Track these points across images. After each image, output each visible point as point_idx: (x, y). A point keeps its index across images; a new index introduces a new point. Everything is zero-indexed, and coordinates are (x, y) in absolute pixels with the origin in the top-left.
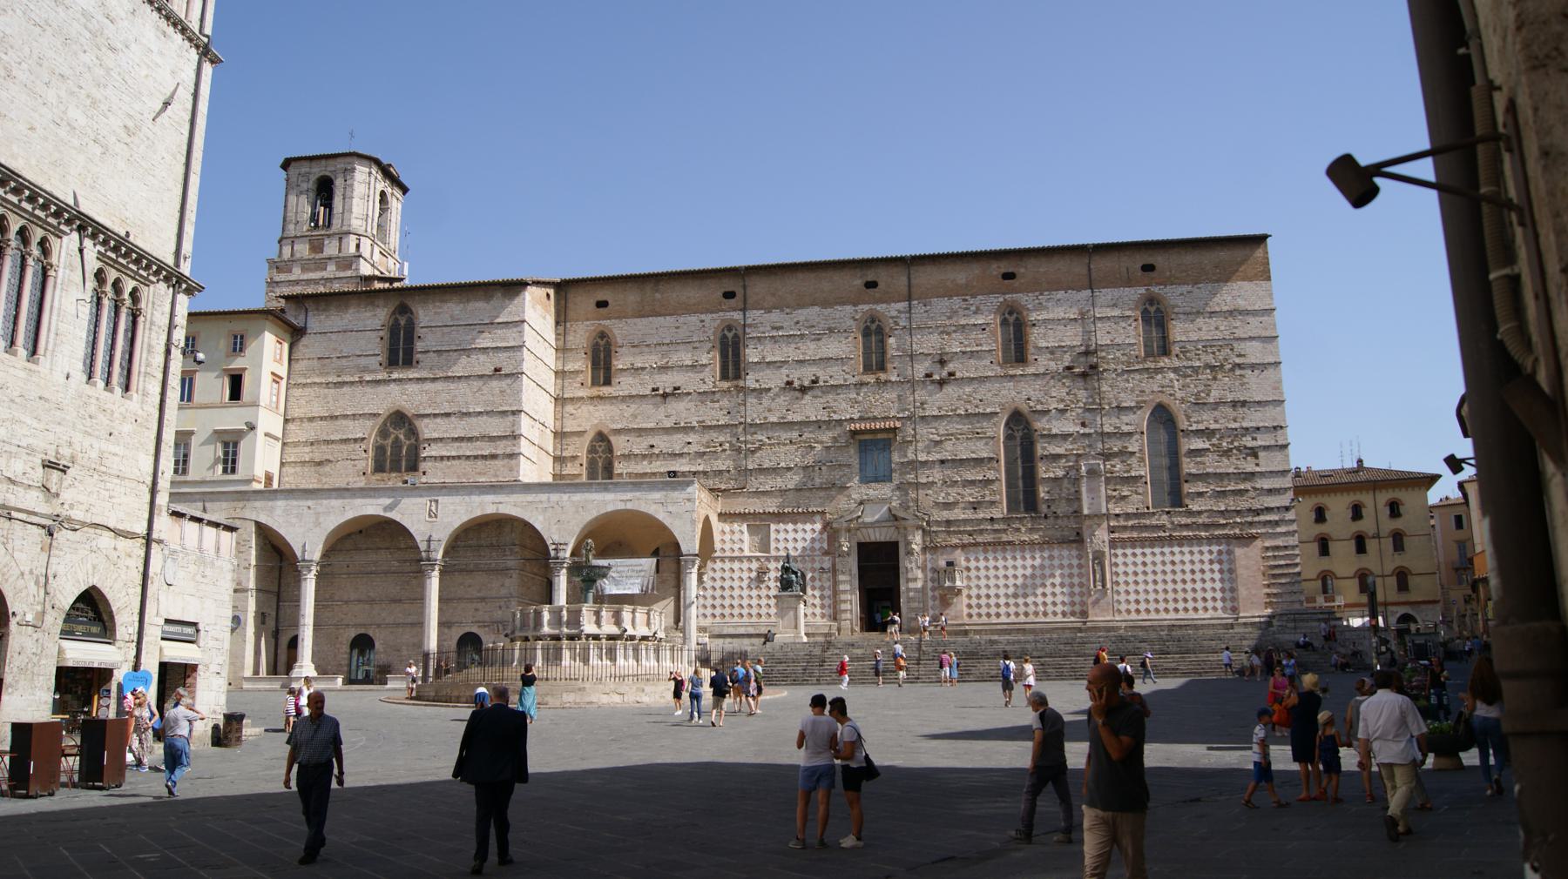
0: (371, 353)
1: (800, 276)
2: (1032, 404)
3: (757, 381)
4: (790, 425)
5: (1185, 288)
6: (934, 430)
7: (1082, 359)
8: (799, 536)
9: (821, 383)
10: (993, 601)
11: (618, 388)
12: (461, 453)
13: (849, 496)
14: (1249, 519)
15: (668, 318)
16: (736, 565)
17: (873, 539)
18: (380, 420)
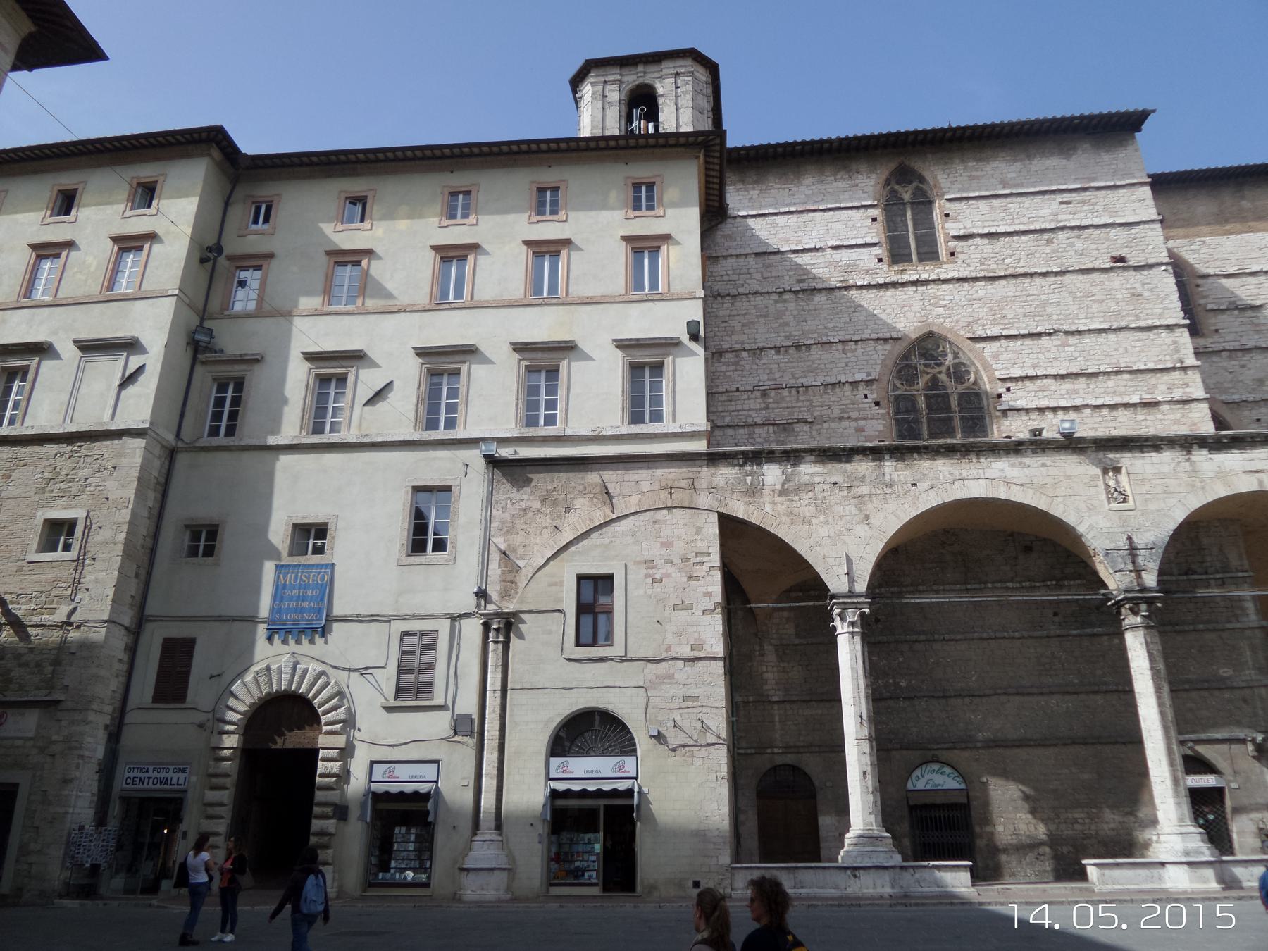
0: (861, 241)
11: (1216, 338)
12: (1078, 402)
18: (899, 348)
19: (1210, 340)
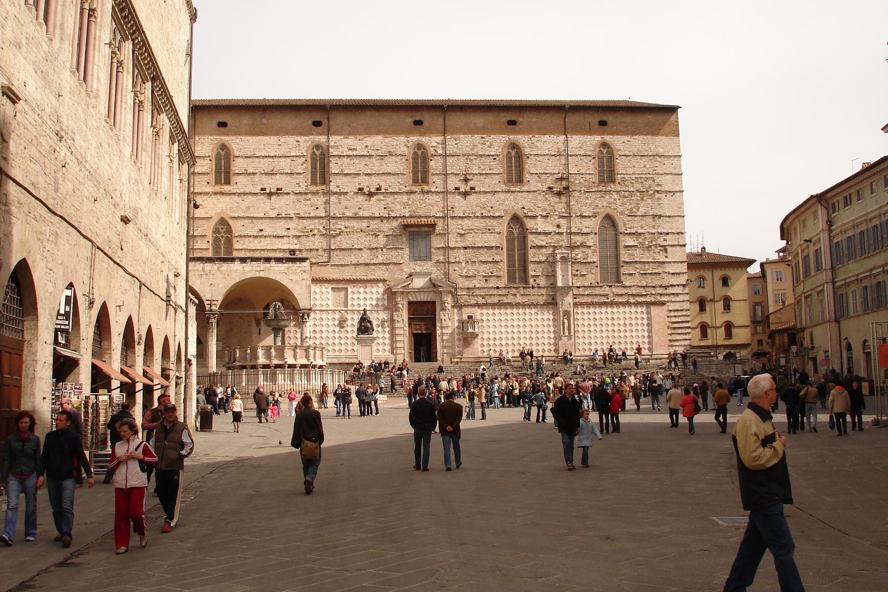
1: (369, 113)
2: (525, 211)
3: (338, 187)
4: (362, 218)
5: (626, 138)
6: (460, 227)
7: (559, 183)
8: (368, 296)
9: (383, 191)
10: (497, 342)
11: (235, 186)
13: (402, 270)
14: (660, 292)
15: (272, 138)
16: (324, 316)
17: (419, 299)
19: (232, 187)
